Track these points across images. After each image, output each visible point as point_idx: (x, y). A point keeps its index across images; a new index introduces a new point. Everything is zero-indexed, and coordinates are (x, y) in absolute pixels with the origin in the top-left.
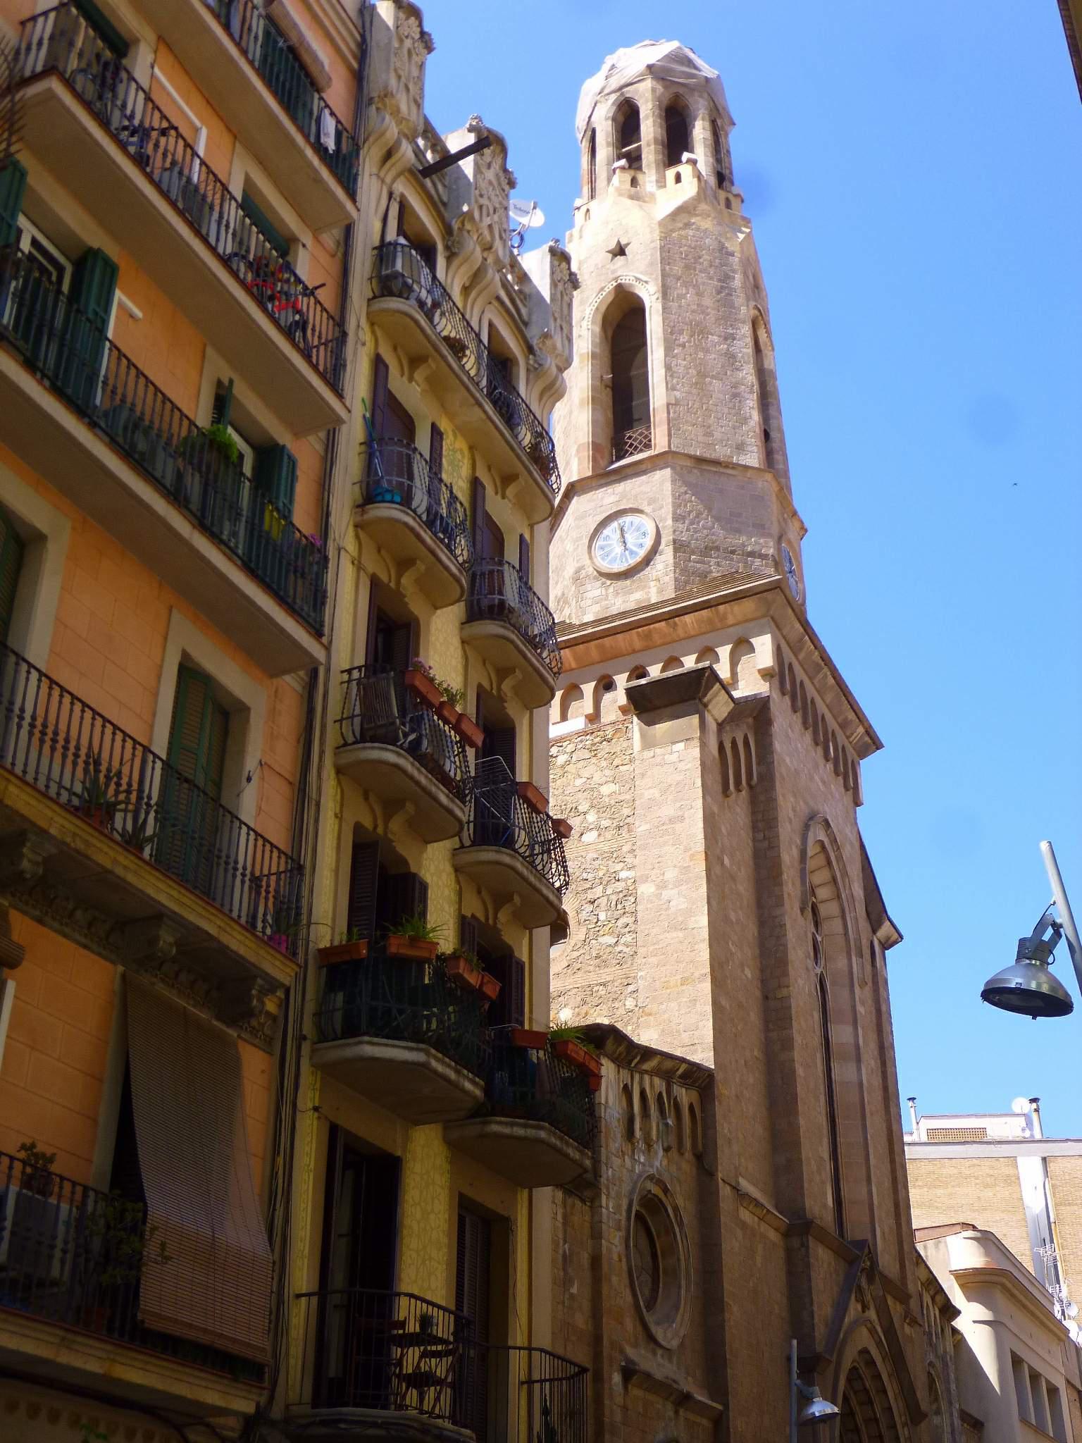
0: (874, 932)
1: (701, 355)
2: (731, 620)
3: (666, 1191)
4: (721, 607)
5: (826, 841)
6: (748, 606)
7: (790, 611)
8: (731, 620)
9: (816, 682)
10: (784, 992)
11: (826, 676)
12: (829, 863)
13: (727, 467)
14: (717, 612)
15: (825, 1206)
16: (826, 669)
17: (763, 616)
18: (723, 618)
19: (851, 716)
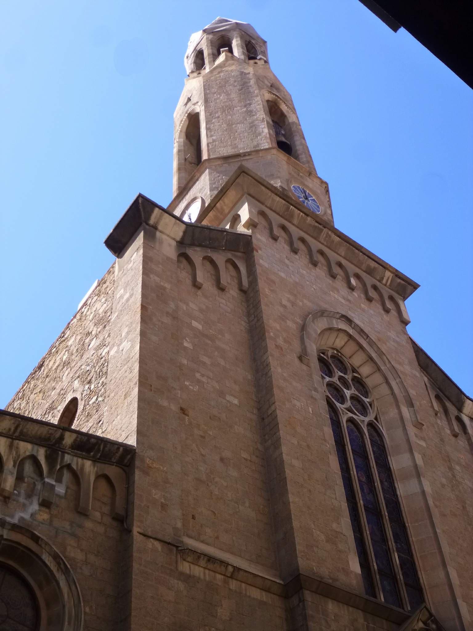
0: (460, 410)
1: (229, 117)
2: (227, 211)
3: (36, 539)
4: (218, 205)
5: (351, 331)
6: (232, 195)
7: (263, 188)
8: (227, 211)
9: (322, 241)
10: (273, 408)
11: (328, 236)
12: (361, 347)
13: (245, 155)
14: (217, 209)
15: (347, 571)
16: (325, 230)
17: (243, 195)
18: (222, 211)
19: (373, 264)
